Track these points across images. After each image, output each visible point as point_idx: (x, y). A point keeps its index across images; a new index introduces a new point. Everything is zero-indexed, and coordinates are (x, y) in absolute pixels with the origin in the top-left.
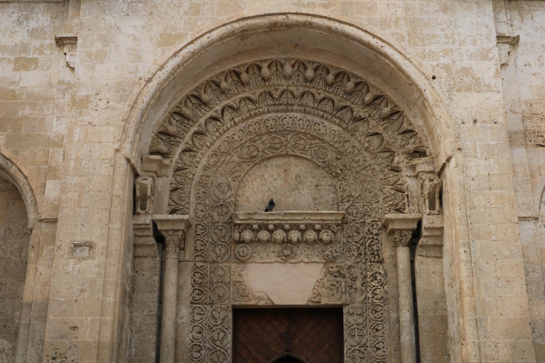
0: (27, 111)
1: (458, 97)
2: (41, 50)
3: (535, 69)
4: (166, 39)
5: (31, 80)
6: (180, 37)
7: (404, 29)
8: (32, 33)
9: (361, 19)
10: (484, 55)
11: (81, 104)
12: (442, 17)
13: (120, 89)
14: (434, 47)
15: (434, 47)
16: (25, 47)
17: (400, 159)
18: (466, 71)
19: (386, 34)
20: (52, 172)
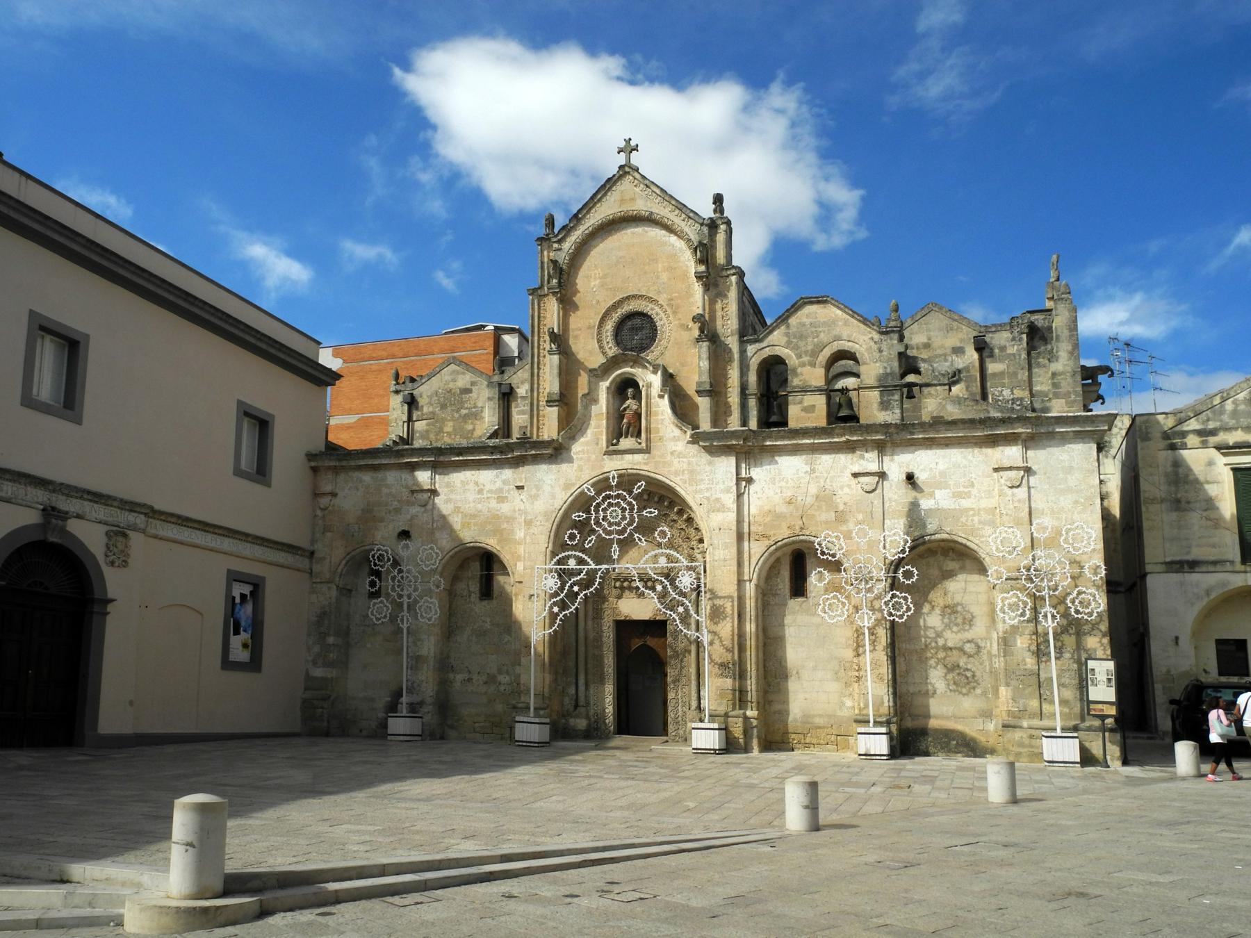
0: (505, 526)
1: (713, 515)
2: (508, 491)
3: (760, 495)
4: (567, 486)
5: (505, 508)
6: (573, 485)
7: (686, 476)
8: (505, 482)
9: (664, 471)
10: (728, 491)
11: (528, 523)
12: (708, 468)
13: (546, 514)
14: (702, 487)
15: (702, 487)
16: (501, 490)
17: (694, 543)
18: (718, 500)
19: (677, 479)
20: (519, 558)
